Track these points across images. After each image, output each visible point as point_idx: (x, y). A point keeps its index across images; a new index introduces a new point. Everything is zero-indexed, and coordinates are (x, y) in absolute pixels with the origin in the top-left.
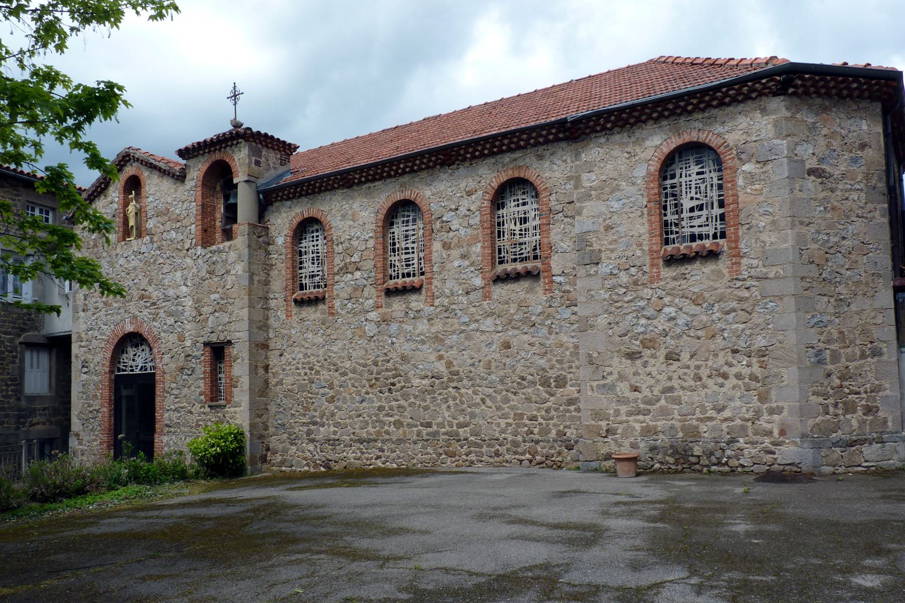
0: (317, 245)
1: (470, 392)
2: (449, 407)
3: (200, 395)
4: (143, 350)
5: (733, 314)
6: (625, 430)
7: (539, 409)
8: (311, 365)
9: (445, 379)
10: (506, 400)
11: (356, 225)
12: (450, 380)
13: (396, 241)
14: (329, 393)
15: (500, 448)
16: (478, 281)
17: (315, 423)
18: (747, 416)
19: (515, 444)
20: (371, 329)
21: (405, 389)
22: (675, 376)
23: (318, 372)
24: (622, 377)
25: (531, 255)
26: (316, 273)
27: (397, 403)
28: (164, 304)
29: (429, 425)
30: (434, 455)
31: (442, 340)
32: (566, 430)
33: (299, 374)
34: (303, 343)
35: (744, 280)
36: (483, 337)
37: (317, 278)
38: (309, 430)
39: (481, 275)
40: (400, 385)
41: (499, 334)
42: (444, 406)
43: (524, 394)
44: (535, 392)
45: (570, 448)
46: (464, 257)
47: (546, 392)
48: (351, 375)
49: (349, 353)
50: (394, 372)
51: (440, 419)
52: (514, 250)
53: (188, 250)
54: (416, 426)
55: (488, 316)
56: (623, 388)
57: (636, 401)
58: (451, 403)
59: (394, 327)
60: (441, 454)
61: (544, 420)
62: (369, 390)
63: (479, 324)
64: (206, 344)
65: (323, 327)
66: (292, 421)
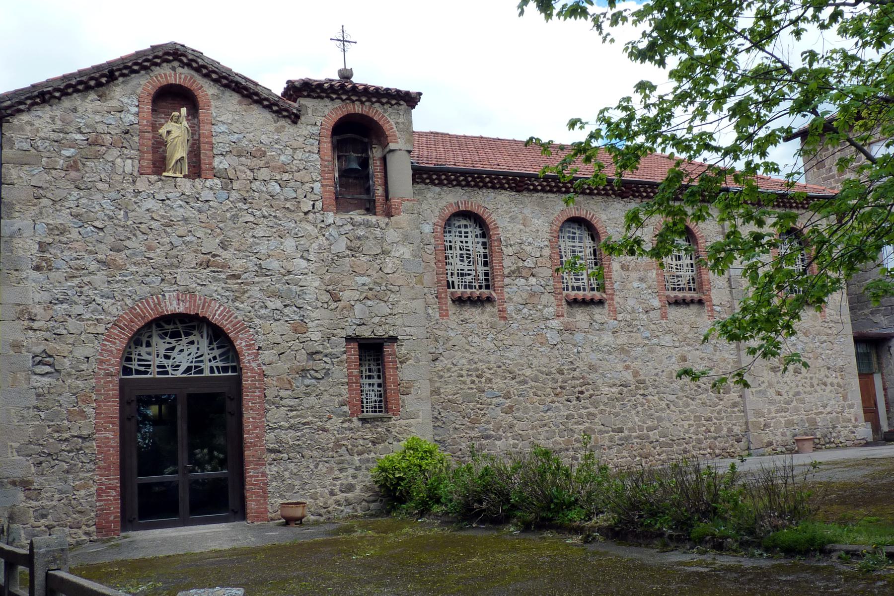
0: (467, 242)
1: (656, 398)
2: (638, 412)
3: (342, 405)
4: (192, 343)
5: (825, 344)
6: (775, 423)
7: (712, 412)
8: (480, 372)
9: (633, 387)
10: (687, 405)
11: (527, 230)
12: (637, 388)
13: (563, 254)
14: (505, 403)
15: (687, 446)
16: (656, 303)
17: (487, 437)
18: (839, 410)
19: (699, 441)
20: (552, 337)
21: (594, 397)
22: (800, 385)
23: (490, 380)
24: (770, 385)
25: (687, 286)
26: (465, 272)
27: (586, 410)
28: (257, 279)
29: (621, 430)
30: (629, 458)
31: (628, 351)
32: (734, 427)
33: (464, 383)
34: (467, 347)
35: (828, 322)
36: (664, 351)
37: (468, 278)
38: (480, 444)
39: (657, 298)
40: (589, 393)
41: (677, 349)
42: (633, 412)
43: (701, 399)
44: (709, 398)
45: (738, 441)
46: (641, 280)
47: (717, 398)
48: (533, 384)
49: (529, 360)
50: (581, 380)
51: (630, 425)
52: (673, 281)
53: (306, 213)
54: (607, 432)
55: (666, 333)
56: (771, 393)
57: (780, 402)
58: (640, 409)
59: (579, 337)
60: (635, 456)
61: (718, 420)
62: (555, 399)
63: (659, 339)
64: (349, 339)
65: (493, 331)
66: (456, 436)
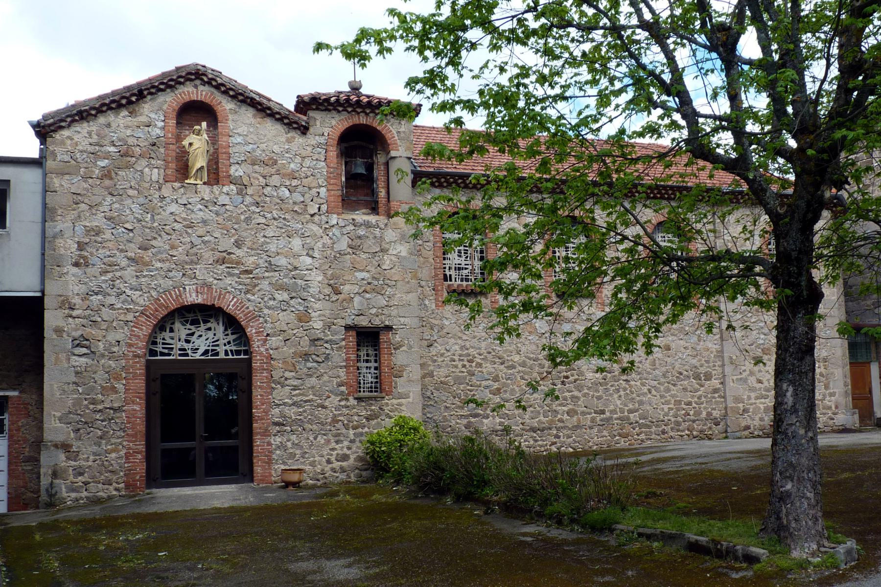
1: (638, 384)
2: (620, 396)
3: (340, 385)
4: (210, 329)
8: (471, 357)
10: (668, 390)
14: (493, 386)
15: (665, 428)
19: (678, 423)
21: (578, 382)
23: (480, 365)
28: (267, 274)
29: (602, 412)
33: (456, 367)
34: (460, 335)
37: (465, 272)
38: (469, 422)
42: (616, 396)
45: (717, 424)
47: (698, 384)
48: (521, 368)
51: (612, 407)
53: (312, 216)
54: (590, 414)
56: (752, 380)
58: (622, 393)
60: (615, 436)
64: (348, 328)
66: (446, 414)
